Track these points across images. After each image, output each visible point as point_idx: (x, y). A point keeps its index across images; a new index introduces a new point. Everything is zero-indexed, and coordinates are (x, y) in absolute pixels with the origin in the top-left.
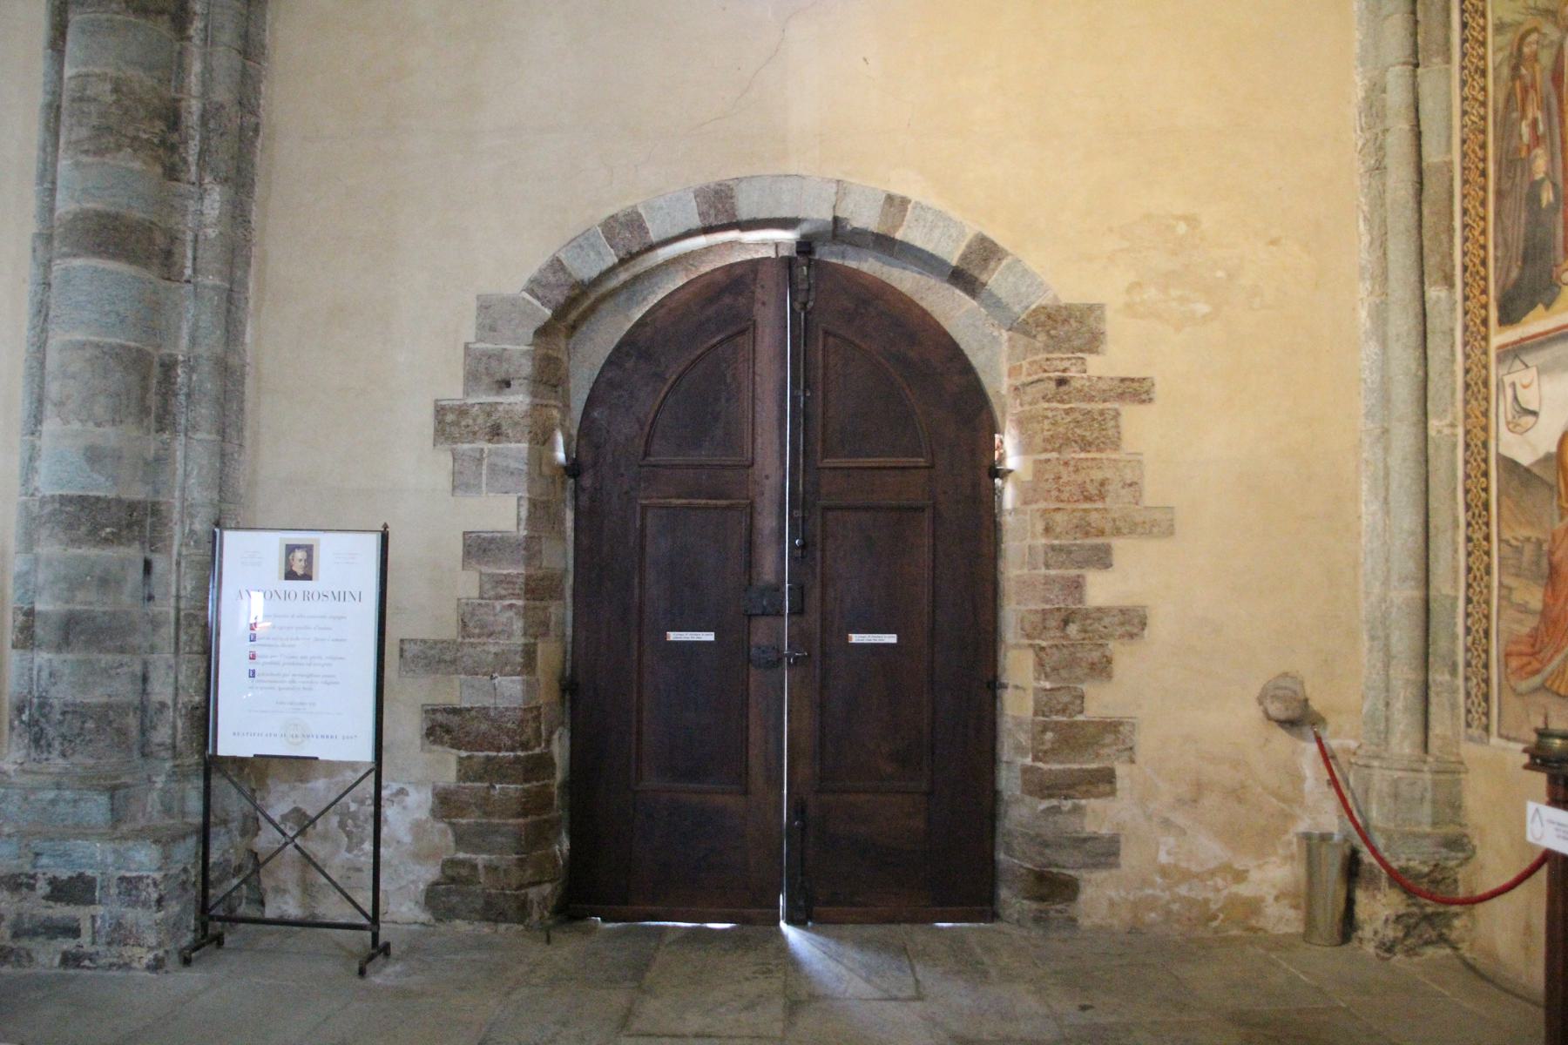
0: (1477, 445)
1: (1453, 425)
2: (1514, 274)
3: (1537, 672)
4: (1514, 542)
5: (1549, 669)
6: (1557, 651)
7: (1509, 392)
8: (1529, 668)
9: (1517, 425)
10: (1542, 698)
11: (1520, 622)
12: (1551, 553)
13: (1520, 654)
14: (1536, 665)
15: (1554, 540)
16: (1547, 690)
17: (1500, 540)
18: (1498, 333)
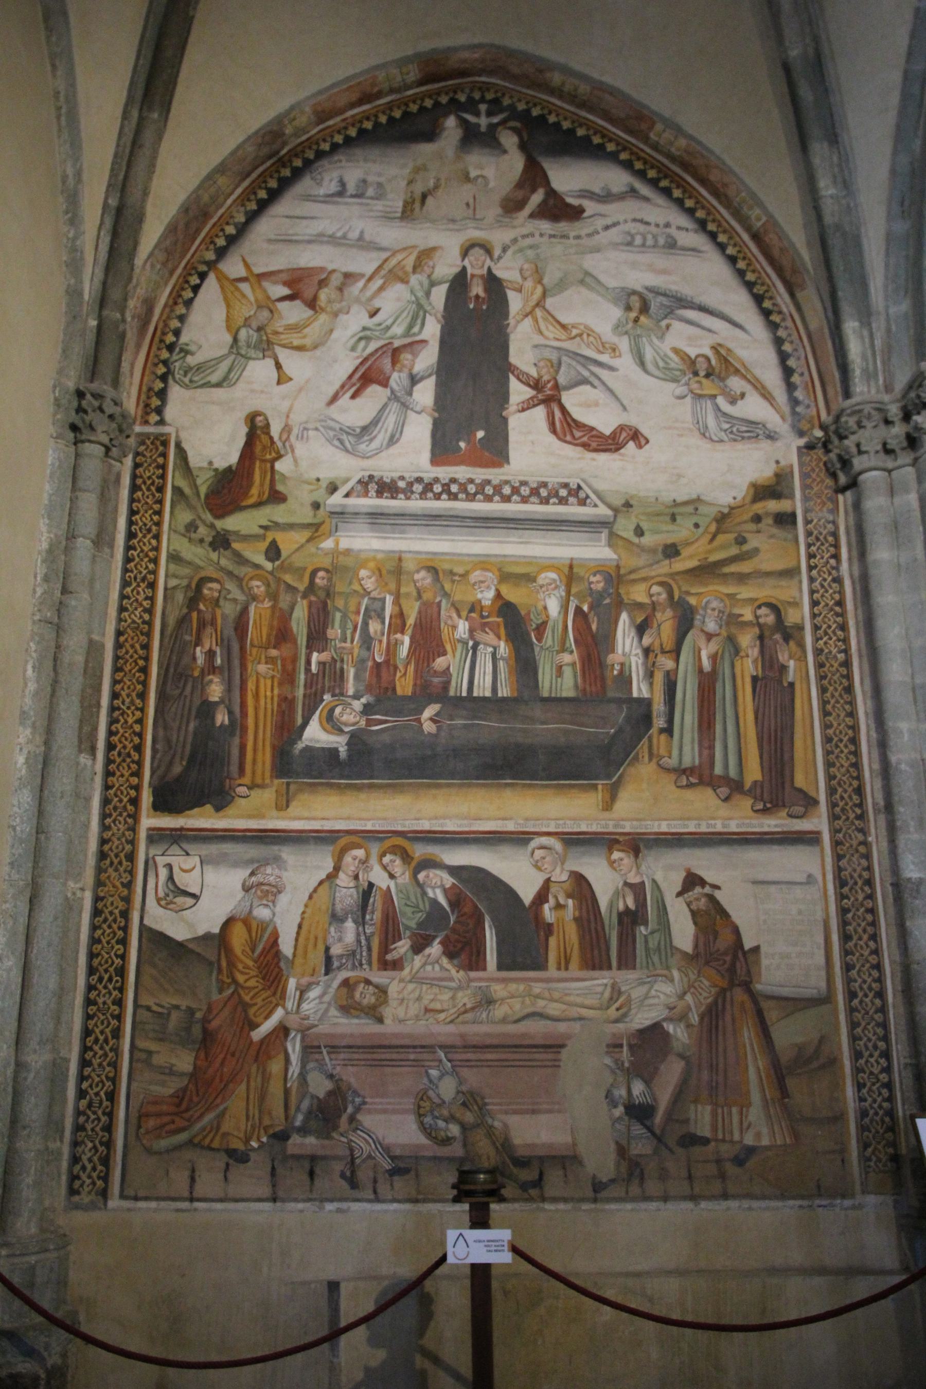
0: (111, 914)
1: (82, 889)
2: (177, 769)
3: (183, 1129)
4: (155, 1008)
5: (198, 1126)
6: (208, 1110)
7: (163, 873)
8: (172, 1127)
9: (172, 902)
10: (189, 1154)
11: (163, 1084)
12: (205, 1021)
13: (159, 1115)
14: (179, 1123)
15: (210, 1009)
16: (195, 1145)
17: (136, 1005)
18: (148, 816)
